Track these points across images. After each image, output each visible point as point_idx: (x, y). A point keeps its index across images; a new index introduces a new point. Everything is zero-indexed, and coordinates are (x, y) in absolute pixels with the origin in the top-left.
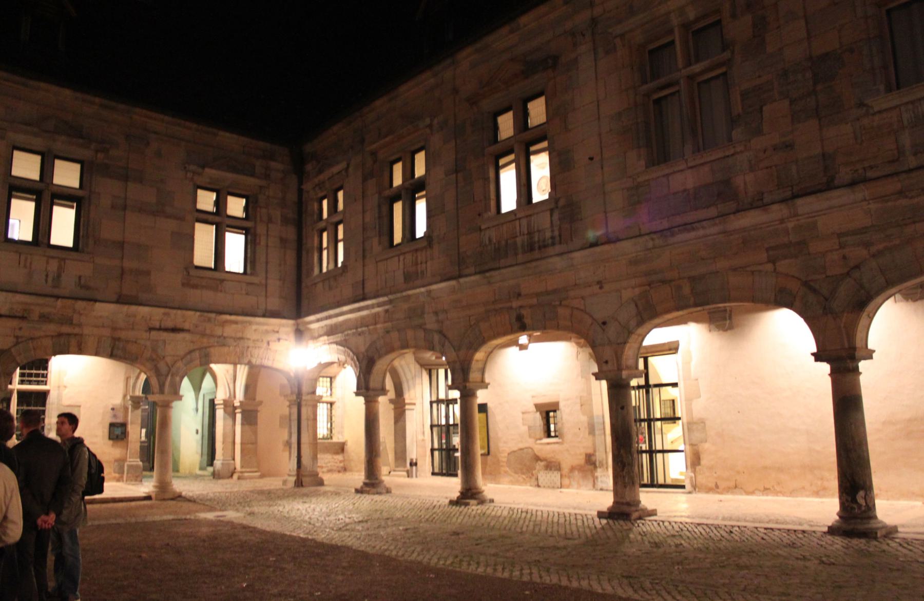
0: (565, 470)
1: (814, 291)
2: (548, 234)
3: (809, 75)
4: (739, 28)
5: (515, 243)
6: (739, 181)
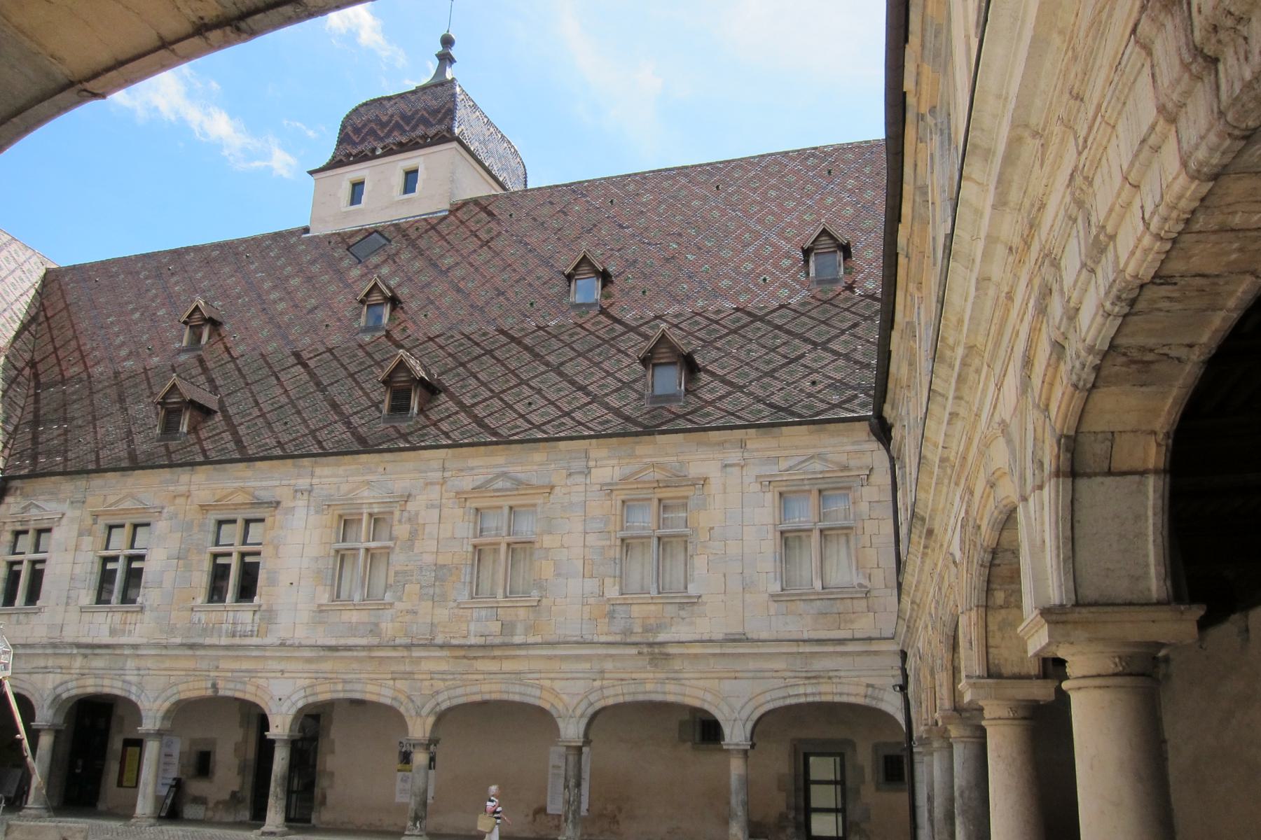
0: (211, 805)
1: (413, 701)
2: (249, 628)
4: (401, 530)
6: (383, 625)
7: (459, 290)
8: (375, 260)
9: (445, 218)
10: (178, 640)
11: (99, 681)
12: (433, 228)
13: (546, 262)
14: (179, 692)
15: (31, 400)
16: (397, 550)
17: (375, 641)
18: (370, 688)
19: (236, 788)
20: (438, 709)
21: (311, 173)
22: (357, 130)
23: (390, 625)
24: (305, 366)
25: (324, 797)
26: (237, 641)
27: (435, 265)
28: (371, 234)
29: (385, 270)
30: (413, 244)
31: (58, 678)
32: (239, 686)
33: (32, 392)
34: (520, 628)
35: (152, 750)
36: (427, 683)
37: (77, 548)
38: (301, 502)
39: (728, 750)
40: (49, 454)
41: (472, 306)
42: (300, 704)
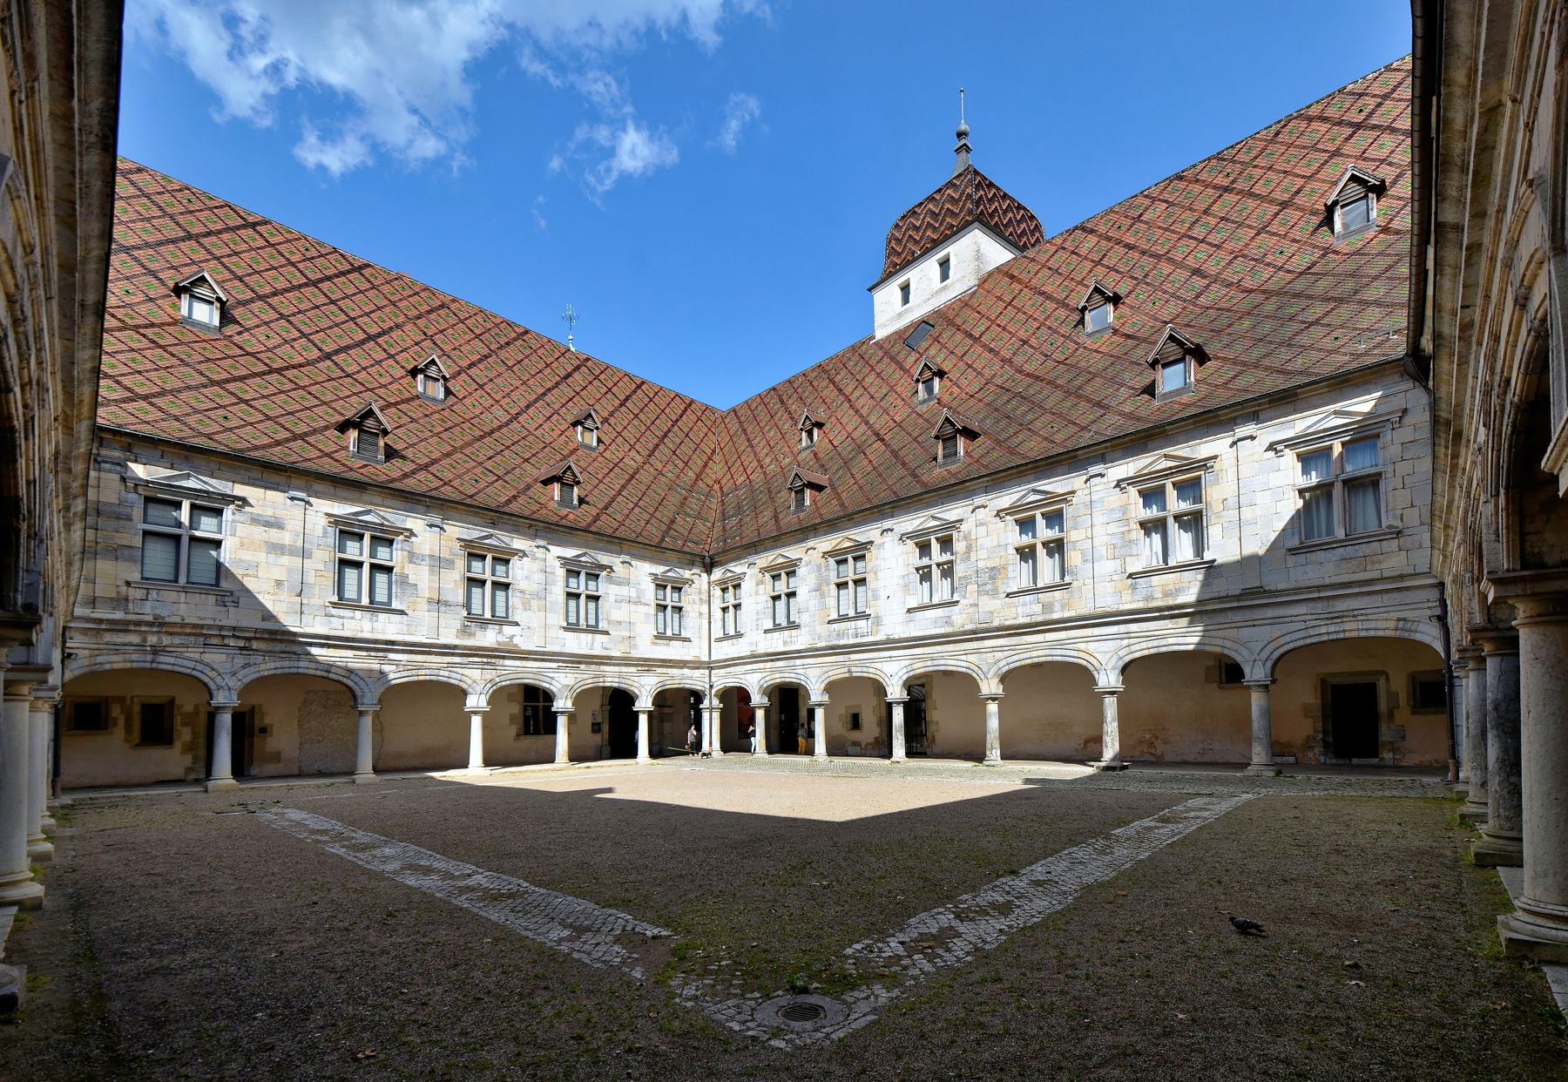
6: (954, 618)
8: (924, 345)
10: (823, 644)
17: (949, 630)
24: (883, 440)
26: (859, 640)
29: (932, 352)
31: (760, 675)
34: (1057, 607)
35: (819, 714)
38: (889, 537)
39: (1249, 687)
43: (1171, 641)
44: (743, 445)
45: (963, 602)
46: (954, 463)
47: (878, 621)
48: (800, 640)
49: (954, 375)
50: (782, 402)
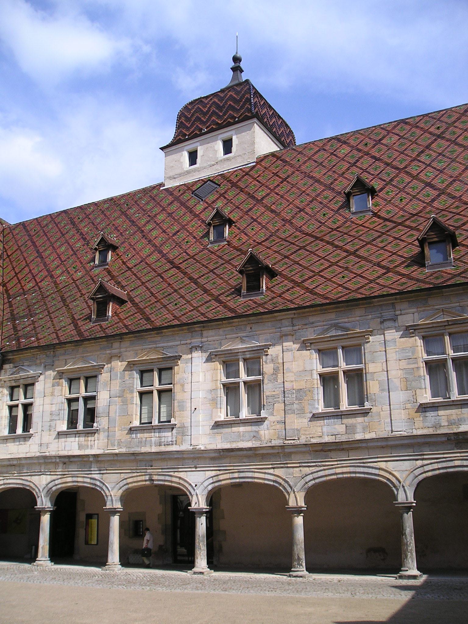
2: (170, 439)
3: (294, 396)
5: (151, 440)
6: (262, 433)
7: (272, 211)
9: (254, 167)
11: (75, 479)
12: (247, 174)
13: (329, 187)
14: (128, 484)
15: (7, 305)
16: (266, 381)
18: (256, 475)
19: (162, 543)
20: (306, 486)
21: (162, 149)
22: (188, 119)
23: (267, 432)
25: (221, 547)
26: (163, 449)
27: (253, 197)
28: (207, 181)
29: (219, 204)
30: (234, 185)
32: (167, 478)
33: (6, 301)
34: (359, 428)
36: (297, 469)
37: (52, 394)
40: (27, 337)
41: (283, 220)
42: (210, 487)
43: (457, 463)
44: (31, 255)
45: (271, 418)
46: (257, 295)
47: (183, 431)
48: (96, 446)
49: (242, 224)
50: (73, 223)
